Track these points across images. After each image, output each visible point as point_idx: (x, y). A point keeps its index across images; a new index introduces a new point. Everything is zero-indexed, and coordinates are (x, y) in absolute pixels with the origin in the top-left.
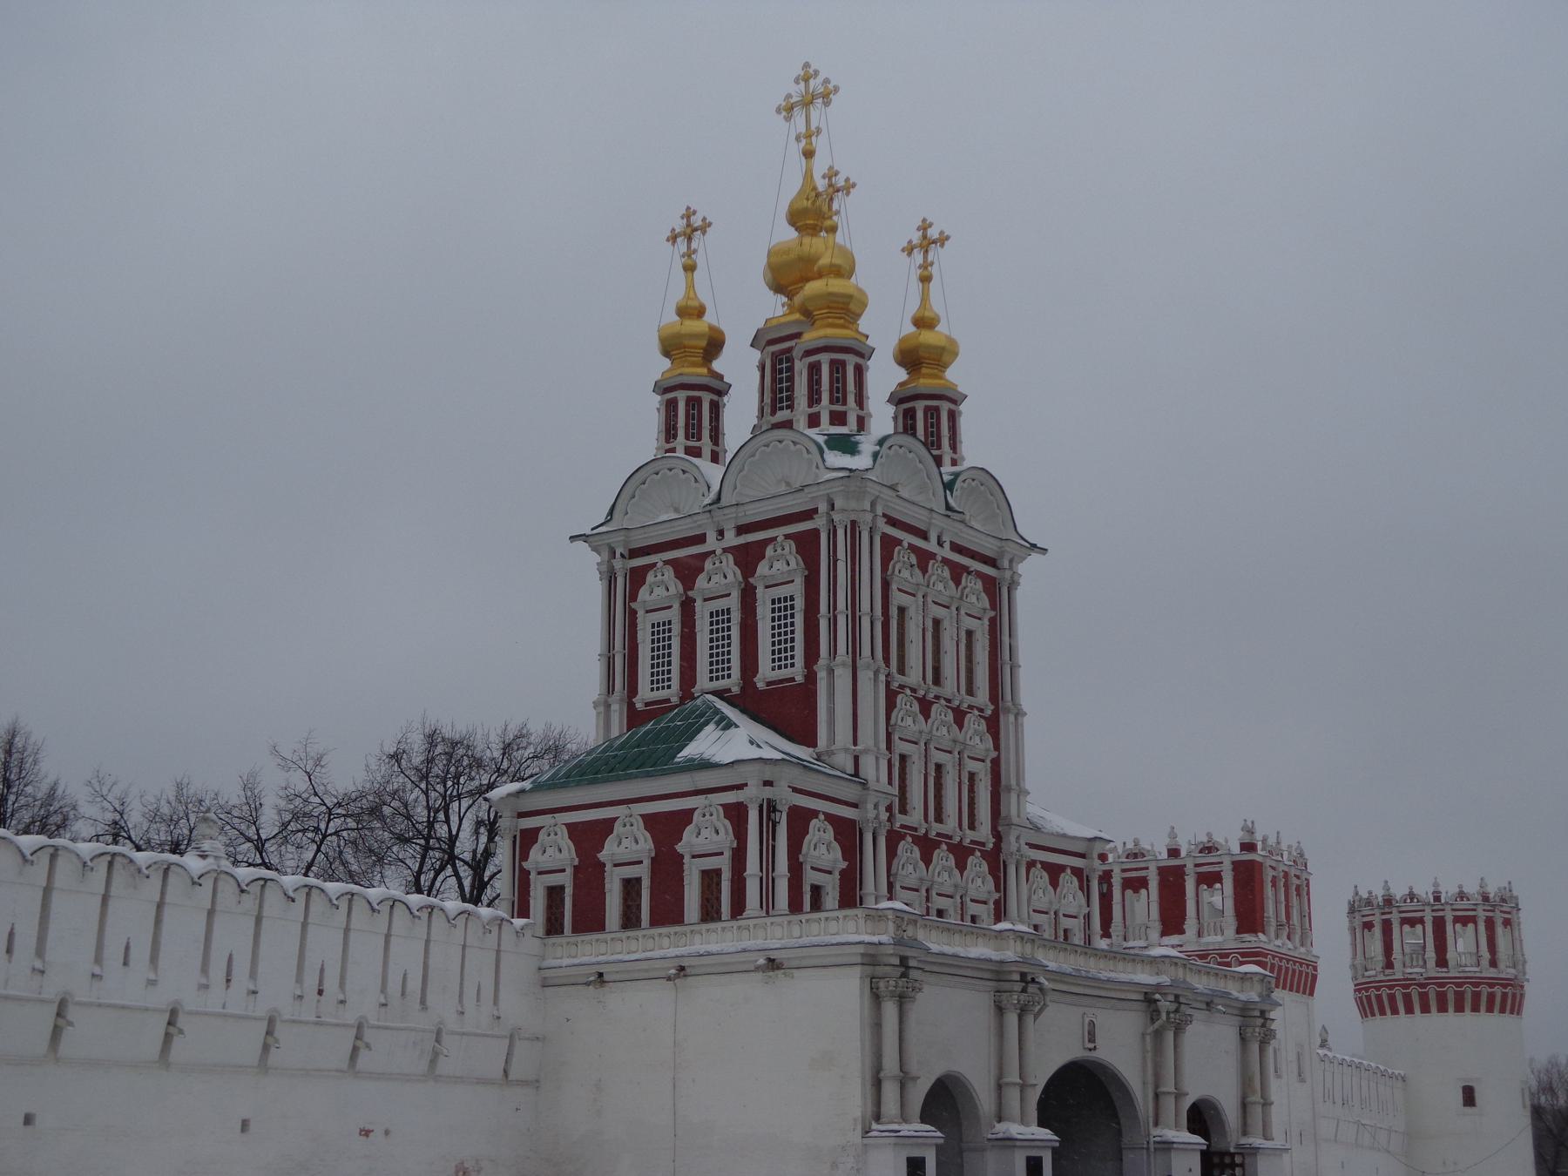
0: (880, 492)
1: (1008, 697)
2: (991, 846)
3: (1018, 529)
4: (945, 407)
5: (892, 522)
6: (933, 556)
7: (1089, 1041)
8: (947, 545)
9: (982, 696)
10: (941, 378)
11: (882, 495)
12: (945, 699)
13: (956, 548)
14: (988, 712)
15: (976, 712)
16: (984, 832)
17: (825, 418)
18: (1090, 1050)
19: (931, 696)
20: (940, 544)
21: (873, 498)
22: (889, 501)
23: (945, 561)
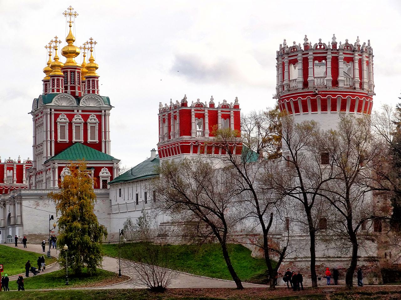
4: (96, 79)
10: (94, 73)
13: (83, 111)
17: (55, 90)
20: (78, 111)
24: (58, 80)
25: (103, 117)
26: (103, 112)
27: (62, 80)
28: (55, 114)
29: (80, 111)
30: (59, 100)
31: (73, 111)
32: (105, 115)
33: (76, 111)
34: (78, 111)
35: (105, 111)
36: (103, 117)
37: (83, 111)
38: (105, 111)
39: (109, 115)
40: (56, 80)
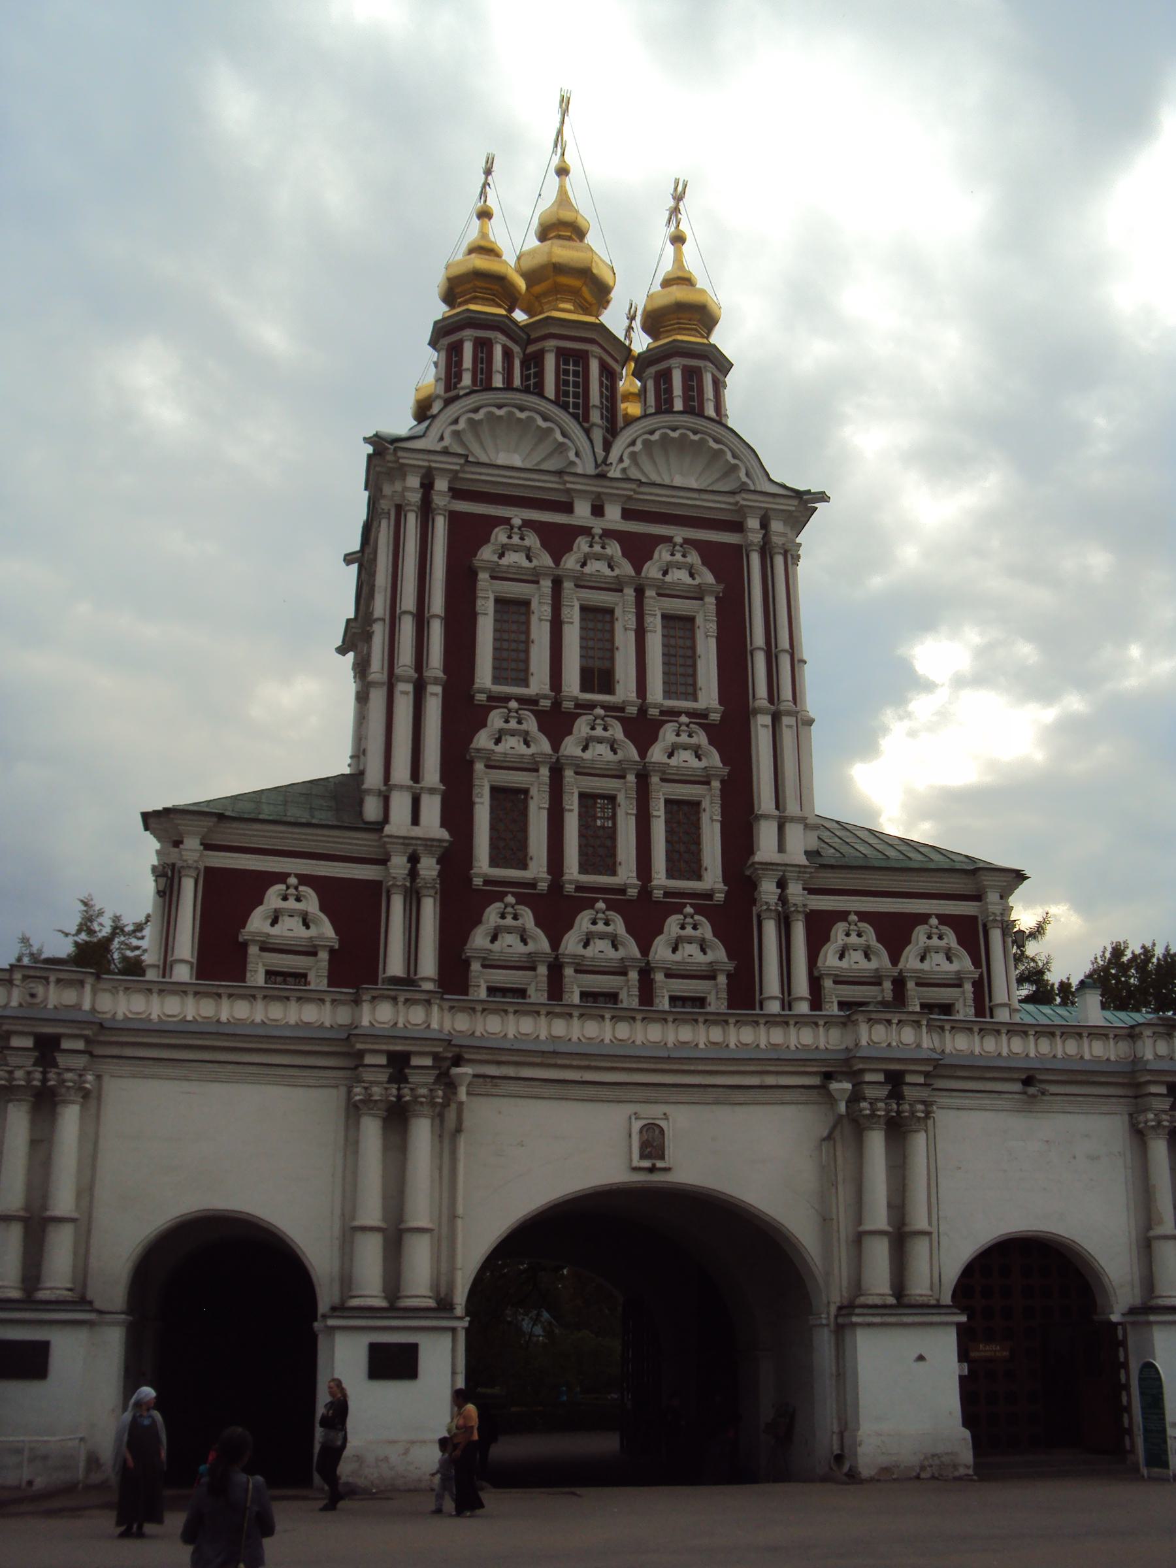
0: (429, 461)
1: (762, 690)
2: (720, 897)
3: (771, 477)
5: (457, 493)
6: (586, 531)
7: (642, 1157)
8: (613, 513)
9: (709, 696)
11: (434, 465)
12: (603, 707)
14: (715, 717)
15: (684, 719)
16: (713, 878)
18: (652, 1170)
19: (568, 705)
20: (598, 511)
21: (423, 471)
22: (456, 472)
23: (608, 534)
24: (483, 347)
25: (755, 559)
26: (753, 523)
27: (508, 354)
28: (455, 519)
29: (613, 513)
30: (477, 436)
31: (568, 508)
32: (766, 551)
33: (582, 512)
34: (598, 511)
35: (765, 525)
36: (755, 559)
37: (627, 514)
38: (765, 525)
39: (791, 556)
40: (468, 349)
